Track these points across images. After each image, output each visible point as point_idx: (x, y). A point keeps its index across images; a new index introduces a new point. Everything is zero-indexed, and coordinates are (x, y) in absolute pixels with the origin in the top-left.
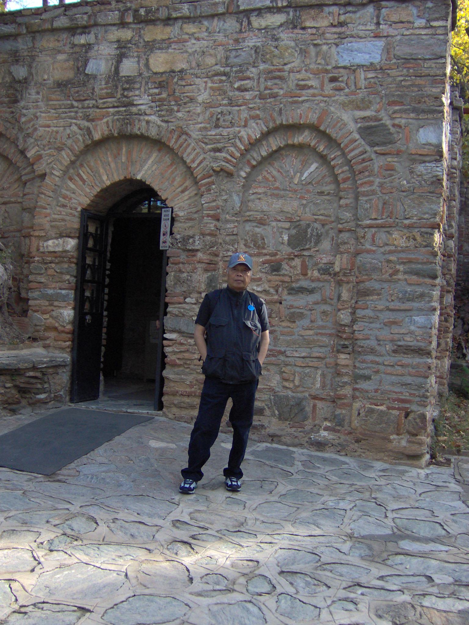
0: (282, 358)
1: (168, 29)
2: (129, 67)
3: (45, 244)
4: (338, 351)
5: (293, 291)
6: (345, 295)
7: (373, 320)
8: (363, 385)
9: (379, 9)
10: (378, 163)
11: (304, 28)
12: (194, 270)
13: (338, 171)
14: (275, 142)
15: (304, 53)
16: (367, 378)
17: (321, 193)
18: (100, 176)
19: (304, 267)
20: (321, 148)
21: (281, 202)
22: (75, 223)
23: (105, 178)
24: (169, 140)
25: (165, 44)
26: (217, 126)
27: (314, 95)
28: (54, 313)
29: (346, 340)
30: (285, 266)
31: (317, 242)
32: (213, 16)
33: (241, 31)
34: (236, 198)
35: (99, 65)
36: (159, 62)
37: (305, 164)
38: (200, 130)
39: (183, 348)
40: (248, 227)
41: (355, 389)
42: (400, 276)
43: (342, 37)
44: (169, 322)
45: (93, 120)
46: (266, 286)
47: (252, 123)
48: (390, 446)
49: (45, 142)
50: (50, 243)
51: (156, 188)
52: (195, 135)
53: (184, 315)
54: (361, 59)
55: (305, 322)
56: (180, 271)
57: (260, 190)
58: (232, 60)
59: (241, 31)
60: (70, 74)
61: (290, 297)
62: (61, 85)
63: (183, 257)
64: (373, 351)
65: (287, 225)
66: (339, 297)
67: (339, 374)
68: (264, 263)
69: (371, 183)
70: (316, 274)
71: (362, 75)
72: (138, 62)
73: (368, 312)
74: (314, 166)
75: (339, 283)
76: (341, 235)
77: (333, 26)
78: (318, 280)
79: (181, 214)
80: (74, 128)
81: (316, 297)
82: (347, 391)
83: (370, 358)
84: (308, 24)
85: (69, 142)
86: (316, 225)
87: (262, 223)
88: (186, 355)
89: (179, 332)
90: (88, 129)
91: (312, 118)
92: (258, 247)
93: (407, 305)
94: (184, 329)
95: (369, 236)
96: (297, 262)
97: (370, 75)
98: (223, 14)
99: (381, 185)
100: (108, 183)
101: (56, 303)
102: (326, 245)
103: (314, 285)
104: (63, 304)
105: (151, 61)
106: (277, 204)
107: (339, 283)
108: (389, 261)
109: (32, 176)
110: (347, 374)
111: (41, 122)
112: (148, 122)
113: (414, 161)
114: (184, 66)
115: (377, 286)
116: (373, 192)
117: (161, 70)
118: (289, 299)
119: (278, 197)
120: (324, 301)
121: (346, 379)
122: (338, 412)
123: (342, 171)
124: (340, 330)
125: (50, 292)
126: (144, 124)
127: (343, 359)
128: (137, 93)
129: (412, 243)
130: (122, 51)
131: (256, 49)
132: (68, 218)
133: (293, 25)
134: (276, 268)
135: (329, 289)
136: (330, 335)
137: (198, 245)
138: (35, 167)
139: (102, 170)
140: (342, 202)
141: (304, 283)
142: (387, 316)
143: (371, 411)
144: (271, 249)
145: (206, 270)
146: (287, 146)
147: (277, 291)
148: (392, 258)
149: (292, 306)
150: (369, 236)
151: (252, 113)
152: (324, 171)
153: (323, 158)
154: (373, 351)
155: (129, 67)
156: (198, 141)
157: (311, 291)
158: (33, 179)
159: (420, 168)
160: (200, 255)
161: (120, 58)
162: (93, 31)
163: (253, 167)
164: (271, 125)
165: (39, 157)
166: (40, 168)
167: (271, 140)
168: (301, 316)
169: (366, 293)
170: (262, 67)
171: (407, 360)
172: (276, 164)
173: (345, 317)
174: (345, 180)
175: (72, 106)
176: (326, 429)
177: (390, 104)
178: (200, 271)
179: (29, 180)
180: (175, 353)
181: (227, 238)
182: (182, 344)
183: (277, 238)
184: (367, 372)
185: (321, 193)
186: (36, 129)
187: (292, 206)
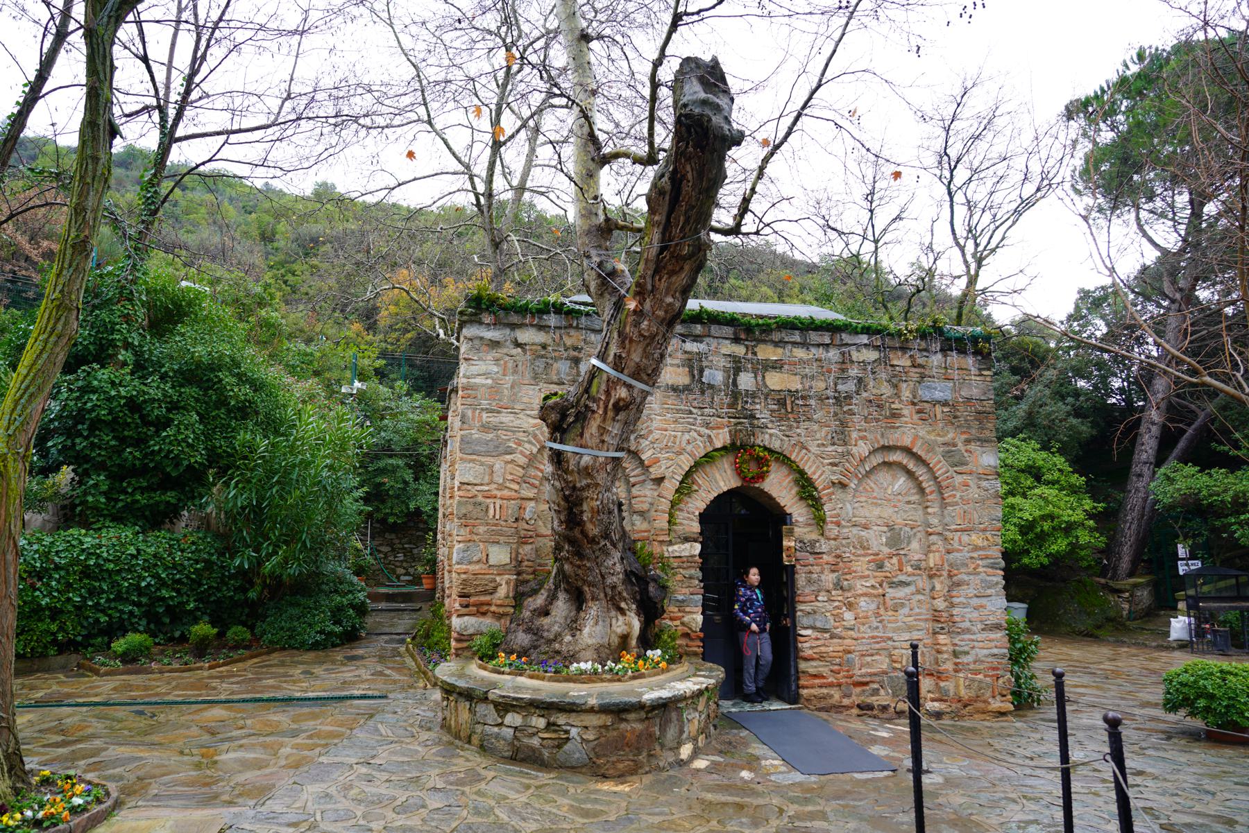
0: (890, 643)
1: (780, 351)
2: (746, 381)
3: (670, 549)
4: (935, 633)
5: (893, 585)
6: (938, 587)
7: (965, 606)
8: (965, 659)
9: (945, 356)
10: (959, 479)
11: (892, 366)
12: (822, 572)
13: (924, 485)
14: (877, 459)
15: (896, 386)
16: (967, 653)
17: (909, 502)
18: (717, 482)
19: (900, 562)
20: (911, 466)
21: (879, 509)
22: (696, 527)
23: (722, 484)
24: (791, 453)
25: (777, 366)
26: (834, 444)
27: (906, 423)
28: (685, 619)
29: (942, 622)
30: (887, 564)
31: (909, 543)
32: (819, 345)
33: (843, 362)
34: (848, 505)
35: (715, 376)
36: (775, 381)
37: (894, 477)
38: (818, 446)
39: (819, 643)
40: (855, 530)
41: (956, 664)
42: (981, 569)
43: (923, 376)
44: (802, 620)
45: (712, 428)
46: (872, 582)
47: (861, 443)
48: (990, 708)
49: (662, 445)
50: (676, 547)
51: (774, 495)
52: (814, 449)
53: (815, 612)
54: (938, 395)
55: (906, 611)
56: (811, 572)
57: (863, 499)
58: (840, 387)
59: (843, 362)
60: (686, 380)
61: (890, 590)
62: (675, 389)
63: (811, 559)
64: (968, 631)
65: (885, 529)
66: (933, 589)
67: (939, 652)
68: (869, 562)
69: (954, 496)
70: (910, 569)
71: (938, 409)
72: (756, 377)
73: (962, 599)
74: (903, 479)
75: (931, 577)
76: (931, 537)
77: (914, 366)
78: (914, 575)
79: (800, 519)
80: (695, 435)
81: (912, 589)
82: (949, 666)
83: (967, 636)
84: (895, 363)
85: (689, 448)
86: (907, 529)
87: (866, 527)
88: (823, 649)
89: (813, 628)
90: (709, 436)
91: (907, 441)
92: (864, 548)
93: (989, 592)
94: (819, 624)
95: (956, 538)
96: (895, 560)
97: (946, 409)
98: (828, 345)
99: (961, 498)
100: (725, 489)
101: (688, 609)
102: (915, 545)
103: (910, 579)
104: (695, 609)
105: (767, 378)
106: (877, 511)
107: (931, 577)
108: (972, 558)
109: (642, 478)
110: (946, 652)
111: (655, 424)
112: (771, 435)
113: (980, 479)
114: (799, 387)
115: (966, 578)
116: (956, 504)
117: (778, 388)
118: (891, 593)
119: (876, 504)
120: (918, 592)
121: (946, 656)
122: (942, 684)
123: (928, 485)
124: (936, 617)
125: (680, 597)
126: (767, 436)
127: (942, 639)
128: (758, 407)
129: (986, 543)
130: (737, 366)
131: (860, 380)
132: (685, 522)
133: (883, 361)
134: (880, 566)
135: (923, 582)
136: (926, 620)
137: (824, 548)
138: (651, 470)
139: (718, 476)
140: (930, 510)
141: (903, 578)
142: (975, 602)
143: (973, 680)
144: (875, 550)
145: (833, 571)
146: (885, 463)
147: (881, 585)
148: (975, 555)
149: (895, 598)
150: (956, 538)
151: (862, 434)
152: (911, 484)
153: (910, 474)
154: (968, 631)
155: (746, 381)
156: (817, 456)
157: (908, 584)
158: (644, 481)
159: (984, 484)
160: (825, 556)
161: (737, 371)
162: (707, 340)
163: (859, 480)
164: (876, 446)
165: (657, 461)
166: (655, 472)
167: (872, 457)
168: (903, 605)
169: (959, 584)
170: (865, 395)
171: (992, 636)
172: (873, 477)
173: (940, 604)
174: (932, 492)
175: (691, 413)
176: (933, 700)
177: (963, 433)
178: (826, 572)
179: (639, 483)
180: (812, 648)
181: (844, 542)
182: (817, 639)
183: (877, 541)
184: (966, 649)
185: (909, 502)
186: (651, 432)
187: (888, 512)
